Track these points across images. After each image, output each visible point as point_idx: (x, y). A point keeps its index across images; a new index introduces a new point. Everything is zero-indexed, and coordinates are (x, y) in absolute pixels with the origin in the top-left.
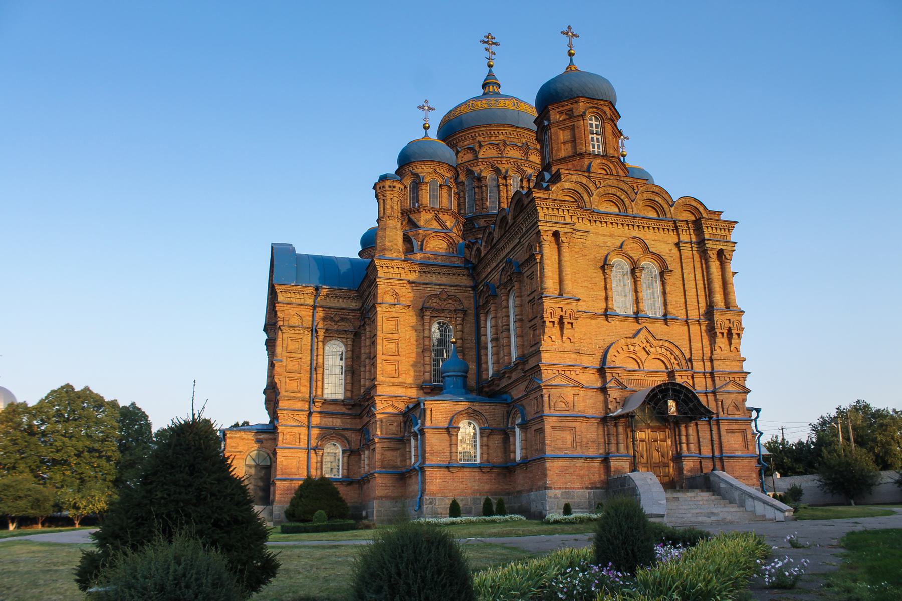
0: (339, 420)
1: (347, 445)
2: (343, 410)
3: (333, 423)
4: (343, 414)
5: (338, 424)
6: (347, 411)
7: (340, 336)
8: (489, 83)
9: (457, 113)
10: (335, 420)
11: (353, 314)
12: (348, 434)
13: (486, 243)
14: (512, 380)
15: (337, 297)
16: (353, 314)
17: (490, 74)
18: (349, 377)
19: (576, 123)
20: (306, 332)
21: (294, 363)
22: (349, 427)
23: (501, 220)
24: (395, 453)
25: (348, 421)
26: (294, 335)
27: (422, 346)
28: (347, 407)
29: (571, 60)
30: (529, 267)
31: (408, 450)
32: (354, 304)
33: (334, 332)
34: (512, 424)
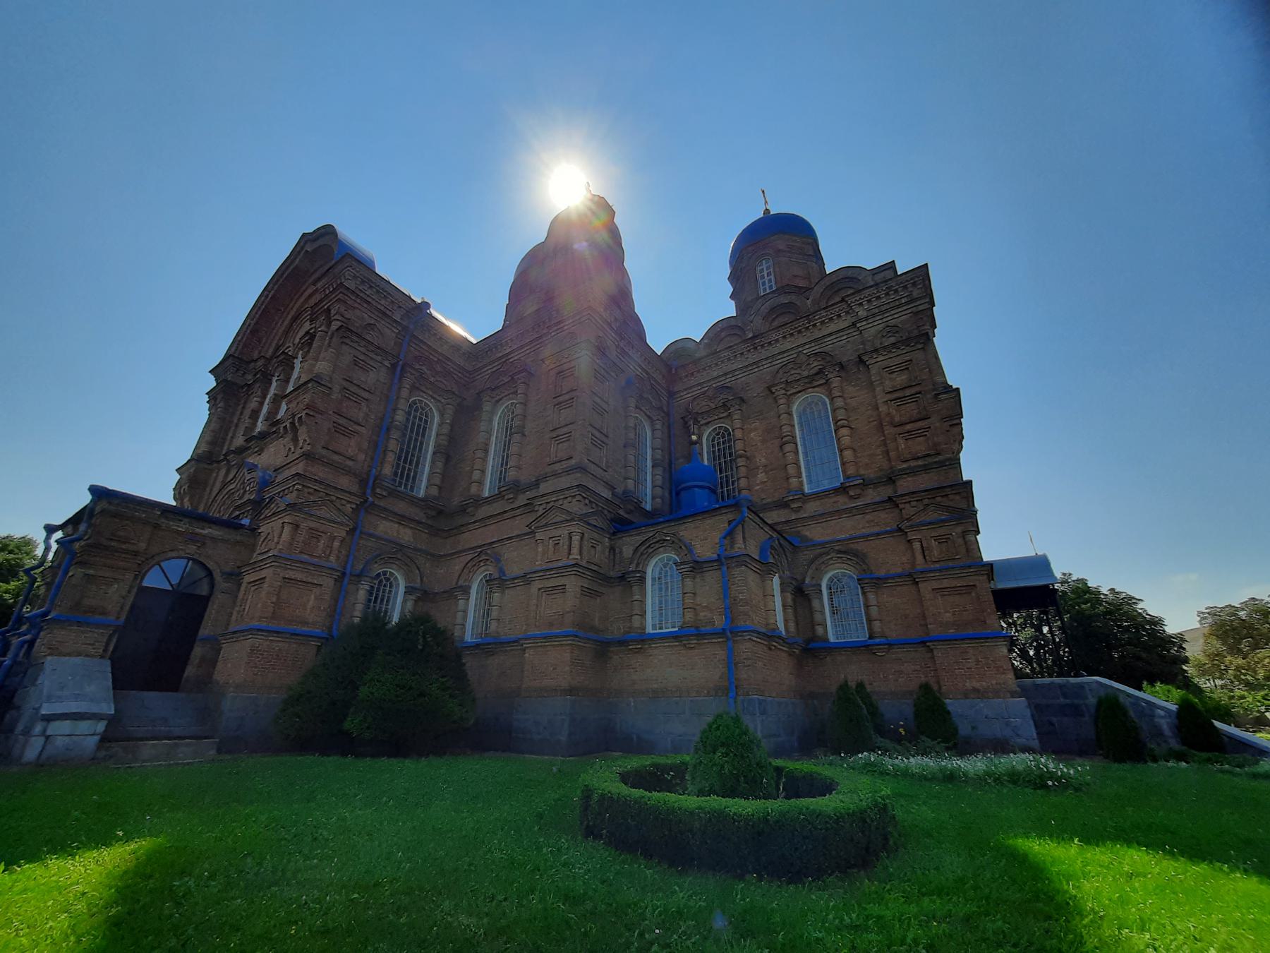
0: (409, 531)
1: (419, 581)
2: (419, 515)
4: (419, 522)
5: (407, 539)
18: (440, 464)
19: (809, 263)
20: (387, 363)
26: (358, 354)
31: (637, 597)
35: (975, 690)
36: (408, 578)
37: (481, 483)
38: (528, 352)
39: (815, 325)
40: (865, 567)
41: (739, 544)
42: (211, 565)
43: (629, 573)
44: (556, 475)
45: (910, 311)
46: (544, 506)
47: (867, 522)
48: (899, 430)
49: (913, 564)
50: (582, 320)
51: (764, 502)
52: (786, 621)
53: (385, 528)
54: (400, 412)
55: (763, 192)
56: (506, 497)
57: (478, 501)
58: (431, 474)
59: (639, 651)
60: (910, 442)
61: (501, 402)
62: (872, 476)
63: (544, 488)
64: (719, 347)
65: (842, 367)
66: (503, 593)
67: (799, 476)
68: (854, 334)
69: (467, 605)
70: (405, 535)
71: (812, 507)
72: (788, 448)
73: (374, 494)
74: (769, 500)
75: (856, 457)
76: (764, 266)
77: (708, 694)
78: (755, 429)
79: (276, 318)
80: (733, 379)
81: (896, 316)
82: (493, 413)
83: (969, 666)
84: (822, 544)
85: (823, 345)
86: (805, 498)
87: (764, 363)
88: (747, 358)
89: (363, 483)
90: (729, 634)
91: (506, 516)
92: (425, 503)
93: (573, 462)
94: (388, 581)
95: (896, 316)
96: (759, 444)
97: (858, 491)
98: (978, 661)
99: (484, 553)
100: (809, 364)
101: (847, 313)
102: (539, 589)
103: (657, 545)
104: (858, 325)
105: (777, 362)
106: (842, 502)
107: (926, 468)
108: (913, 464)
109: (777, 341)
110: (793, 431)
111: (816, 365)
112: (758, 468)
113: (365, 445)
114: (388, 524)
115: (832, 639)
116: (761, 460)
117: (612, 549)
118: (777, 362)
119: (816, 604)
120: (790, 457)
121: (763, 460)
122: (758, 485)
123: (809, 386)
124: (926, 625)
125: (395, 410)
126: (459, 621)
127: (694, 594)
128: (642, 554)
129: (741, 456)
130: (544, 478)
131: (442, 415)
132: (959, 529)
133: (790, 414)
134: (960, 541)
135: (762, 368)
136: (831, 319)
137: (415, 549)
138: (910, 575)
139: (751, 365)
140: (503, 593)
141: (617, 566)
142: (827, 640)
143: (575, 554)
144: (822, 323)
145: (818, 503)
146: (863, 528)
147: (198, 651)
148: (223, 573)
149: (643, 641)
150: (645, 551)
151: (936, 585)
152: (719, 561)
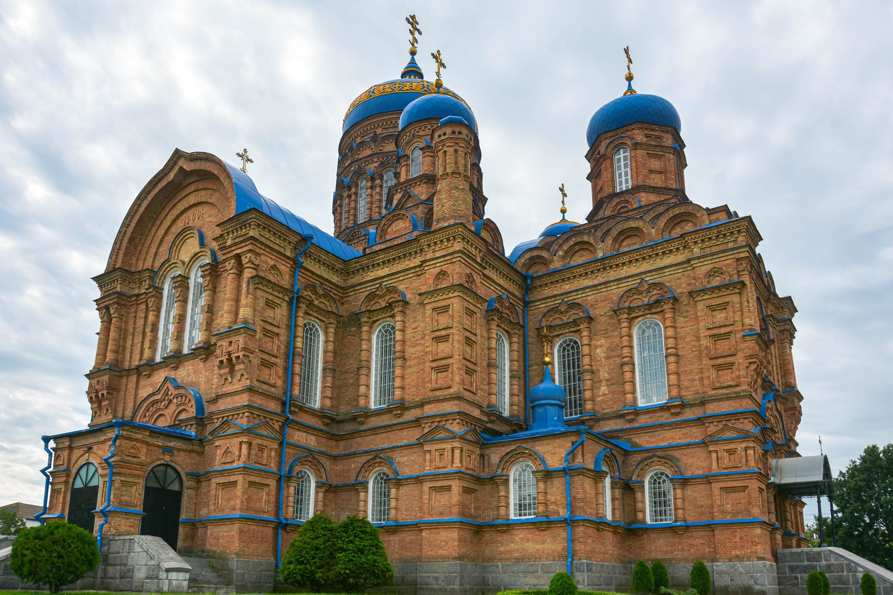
0: (313, 438)
3: (307, 440)
4: (321, 430)
6: (322, 427)
7: (320, 317)
10: (309, 438)
11: (335, 292)
12: (323, 460)
13: (566, 252)
14: (635, 425)
15: (319, 261)
16: (335, 292)
18: (329, 379)
19: (666, 155)
21: (267, 339)
22: (324, 449)
24: (469, 497)
25: (324, 440)
26: (270, 297)
27: (486, 358)
28: (326, 420)
29: (630, 85)
30: (714, 295)
31: (502, 494)
32: (336, 279)
33: (315, 309)
35: (737, 556)
36: (318, 476)
37: (367, 396)
38: (401, 278)
40: (676, 469)
41: (579, 459)
42: (178, 468)
43: (496, 476)
44: (438, 400)
46: (430, 424)
47: (683, 434)
49: (710, 470)
50: (454, 260)
51: (605, 411)
52: (613, 510)
53: (298, 437)
54: (299, 339)
55: (627, 51)
56: (394, 413)
57: (368, 414)
58: (324, 388)
59: (504, 532)
60: (720, 373)
61: (378, 323)
62: (690, 397)
64: (574, 258)
65: (675, 299)
66: (398, 489)
67: (634, 392)
69: (366, 496)
70: (311, 441)
71: (643, 420)
72: (626, 368)
73: (290, 412)
74: (608, 411)
75: (679, 381)
76: (622, 156)
77: (554, 560)
78: (601, 346)
79: (150, 226)
80: (584, 295)
82: (370, 333)
83: (735, 540)
84: (648, 451)
85: (661, 275)
86: (638, 412)
87: (611, 284)
88: (597, 276)
89: (284, 404)
90: (570, 523)
91: (394, 428)
92: (321, 414)
93: (452, 390)
94: (302, 478)
96: (603, 360)
97: (678, 410)
98: (741, 538)
99: (377, 457)
100: (649, 292)
102: (430, 488)
105: (623, 285)
106: (666, 418)
109: (624, 264)
110: (632, 353)
111: (655, 294)
112: (601, 381)
113: (281, 371)
114: (298, 433)
116: (604, 374)
117: (482, 456)
118: (623, 285)
120: (628, 375)
121: (606, 375)
122: (600, 396)
123: (648, 312)
124: (713, 513)
125: (295, 337)
126: (362, 508)
127: (546, 493)
128: (506, 462)
129: (587, 371)
131: (326, 333)
132: (744, 445)
133: (630, 336)
134: (743, 453)
135: (609, 289)
137: (320, 453)
138: (707, 477)
139: (600, 284)
140: (398, 489)
141: (486, 469)
143: (457, 463)
145: (648, 416)
146: (679, 439)
147: (181, 530)
148: (187, 475)
149: (508, 527)
150: (509, 459)
151: (723, 485)
152: (565, 471)
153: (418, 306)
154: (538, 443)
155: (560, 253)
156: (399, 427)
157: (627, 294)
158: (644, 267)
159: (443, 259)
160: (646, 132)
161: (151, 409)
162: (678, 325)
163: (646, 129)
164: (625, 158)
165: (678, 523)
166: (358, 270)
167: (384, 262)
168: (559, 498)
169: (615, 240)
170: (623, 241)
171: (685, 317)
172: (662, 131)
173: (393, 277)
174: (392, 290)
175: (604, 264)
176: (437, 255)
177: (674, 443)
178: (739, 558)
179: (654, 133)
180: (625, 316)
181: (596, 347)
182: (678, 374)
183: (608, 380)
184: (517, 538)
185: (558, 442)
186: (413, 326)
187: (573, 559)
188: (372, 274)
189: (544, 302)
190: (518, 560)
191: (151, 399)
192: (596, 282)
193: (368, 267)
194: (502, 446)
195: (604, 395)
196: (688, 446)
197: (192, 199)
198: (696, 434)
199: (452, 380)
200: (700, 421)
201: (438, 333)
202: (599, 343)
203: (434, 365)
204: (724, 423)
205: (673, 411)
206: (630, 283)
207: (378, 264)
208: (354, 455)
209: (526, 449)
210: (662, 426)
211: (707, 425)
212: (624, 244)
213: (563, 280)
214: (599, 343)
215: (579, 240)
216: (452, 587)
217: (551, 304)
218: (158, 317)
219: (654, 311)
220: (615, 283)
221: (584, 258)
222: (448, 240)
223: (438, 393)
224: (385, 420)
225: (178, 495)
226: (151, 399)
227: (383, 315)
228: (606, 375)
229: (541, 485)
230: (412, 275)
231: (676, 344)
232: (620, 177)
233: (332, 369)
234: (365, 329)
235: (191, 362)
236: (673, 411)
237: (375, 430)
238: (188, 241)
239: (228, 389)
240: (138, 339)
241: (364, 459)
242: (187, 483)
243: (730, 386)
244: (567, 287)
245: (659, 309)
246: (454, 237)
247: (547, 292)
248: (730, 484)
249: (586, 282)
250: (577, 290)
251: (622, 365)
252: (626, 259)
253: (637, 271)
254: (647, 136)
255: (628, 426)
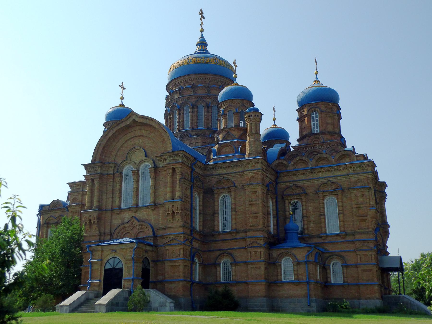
0: (197, 244)
1: (202, 261)
6: (200, 239)
8: (203, 43)
9: (207, 61)
17: (202, 37)
18: (202, 218)
23: (319, 158)
29: (317, 77)
34: (328, 263)
38: (232, 176)
39: (335, 170)
45: (366, 176)
48: (358, 218)
49: (357, 262)
50: (258, 172)
52: (320, 277)
60: (361, 223)
63: (249, 234)
65: (343, 191)
67: (325, 227)
68: (348, 178)
72: (322, 217)
76: (315, 115)
77: (302, 298)
78: (310, 206)
80: (303, 183)
81: (362, 176)
84: (332, 252)
86: (327, 236)
87: (315, 180)
88: (309, 175)
90: (308, 283)
93: (259, 227)
95: (362, 176)
96: (312, 212)
100: (331, 185)
101: (346, 169)
102: (251, 267)
103: (285, 255)
104: (349, 176)
106: (339, 239)
107: (364, 233)
108: (361, 231)
109: (320, 172)
111: (334, 187)
112: (311, 221)
115: (332, 282)
116: (312, 218)
117: (269, 254)
119: (328, 271)
120: (323, 220)
122: (310, 228)
123: (331, 194)
124: (359, 280)
127: (298, 271)
130: (249, 231)
132: (370, 253)
133: (323, 203)
134: (370, 256)
135: (314, 182)
136: (340, 169)
138: (356, 265)
141: (271, 260)
142: (330, 282)
144: (337, 170)
148: (151, 261)
150: (281, 256)
151: (362, 269)
152: (306, 262)
153: (241, 189)
154: (293, 250)
155: (292, 163)
156: (235, 240)
157: (322, 185)
158: (329, 174)
159: (253, 171)
160: (326, 106)
161: (122, 230)
162: (344, 201)
163: (326, 104)
164: (316, 117)
165: (345, 284)
166: (211, 169)
167: (224, 168)
168: (303, 273)
169: (316, 161)
170: (320, 161)
171: (347, 198)
172: (333, 105)
173: (228, 175)
174: (229, 181)
175: (312, 171)
176: (250, 169)
177: (342, 250)
178: (369, 298)
179: (329, 106)
180: (321, 195)
181: (309, 206)
182: (344, 222)
183: (314, 221)
184: (286, 289)
185: (301, 250)
186: (239, 198)
187: (310, 298)
188: (218, 171)
189: (285, 183)
190: (286, 297)
191: (124, 226)
192: (308, 178)
193: (216, 168)
194: (277, 250)
195: (312, 227)
196: (348, 251)
197: (138, 133)
198: (351, 247)
199: (259, 223)
200: (353, 242)
201: (252, 203)
202: (310, 205)
203: (251, 215)
204: (363, 243)
205: (342, 237)
206: (323, 181)
207: (221, 168)
208: (213, 251)
209: (289, 252)
210: (337, 243)
211: (356, 244)
212: (320, 163)
213: (293, 175)
214: (310, 205)
215: (301, 158)
216: (264, 308)
217: (288, 184)
218: (121, 186)
219: (333, 194)
220: (317, 180)
221: (302, 166)
222: (255, 163)
223: (253, 228)
224: (228, 237)
225: (149, 270)
226: (124, 226)
227: (224, 191)
228: (313, 219)
229: (296, 267)
230: (238, 175)
231: (343, 209)
232: (314, 125)
233: (203, 213)
234: (216, 196)
235: (145, 210)
236: (342, 237)
237: (223, 241)
238: (136, 152)
239: (170, 225)
240: (110, 196)
241: (217, 253)
242: (151, 264)
243: (365, 229)
244: (295, 178)
245: (336, 193)
246: (258, 163)
247: (286, 179)
248: (365, 268)
249: (303, 177)
250: (300, 181)
251: (321, 215)
252: (322, 170)
253: (326, 176)
254: (326, 107)
255: (323, 241)
